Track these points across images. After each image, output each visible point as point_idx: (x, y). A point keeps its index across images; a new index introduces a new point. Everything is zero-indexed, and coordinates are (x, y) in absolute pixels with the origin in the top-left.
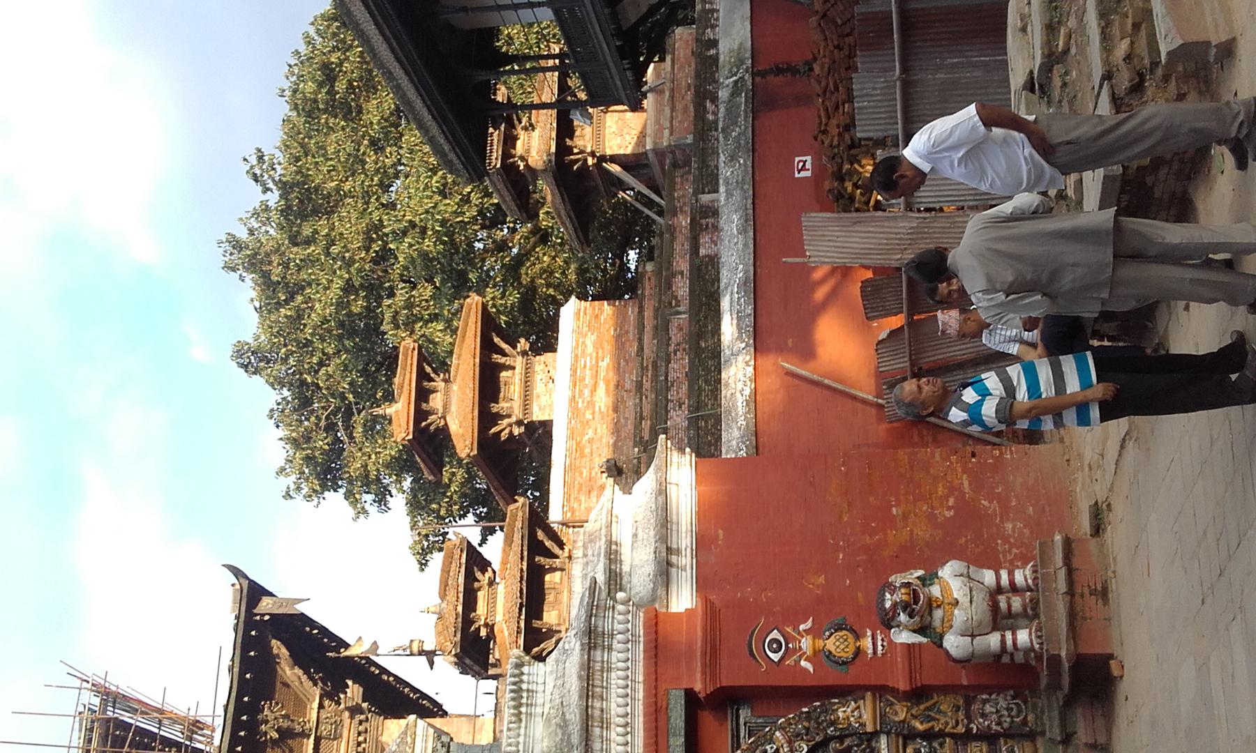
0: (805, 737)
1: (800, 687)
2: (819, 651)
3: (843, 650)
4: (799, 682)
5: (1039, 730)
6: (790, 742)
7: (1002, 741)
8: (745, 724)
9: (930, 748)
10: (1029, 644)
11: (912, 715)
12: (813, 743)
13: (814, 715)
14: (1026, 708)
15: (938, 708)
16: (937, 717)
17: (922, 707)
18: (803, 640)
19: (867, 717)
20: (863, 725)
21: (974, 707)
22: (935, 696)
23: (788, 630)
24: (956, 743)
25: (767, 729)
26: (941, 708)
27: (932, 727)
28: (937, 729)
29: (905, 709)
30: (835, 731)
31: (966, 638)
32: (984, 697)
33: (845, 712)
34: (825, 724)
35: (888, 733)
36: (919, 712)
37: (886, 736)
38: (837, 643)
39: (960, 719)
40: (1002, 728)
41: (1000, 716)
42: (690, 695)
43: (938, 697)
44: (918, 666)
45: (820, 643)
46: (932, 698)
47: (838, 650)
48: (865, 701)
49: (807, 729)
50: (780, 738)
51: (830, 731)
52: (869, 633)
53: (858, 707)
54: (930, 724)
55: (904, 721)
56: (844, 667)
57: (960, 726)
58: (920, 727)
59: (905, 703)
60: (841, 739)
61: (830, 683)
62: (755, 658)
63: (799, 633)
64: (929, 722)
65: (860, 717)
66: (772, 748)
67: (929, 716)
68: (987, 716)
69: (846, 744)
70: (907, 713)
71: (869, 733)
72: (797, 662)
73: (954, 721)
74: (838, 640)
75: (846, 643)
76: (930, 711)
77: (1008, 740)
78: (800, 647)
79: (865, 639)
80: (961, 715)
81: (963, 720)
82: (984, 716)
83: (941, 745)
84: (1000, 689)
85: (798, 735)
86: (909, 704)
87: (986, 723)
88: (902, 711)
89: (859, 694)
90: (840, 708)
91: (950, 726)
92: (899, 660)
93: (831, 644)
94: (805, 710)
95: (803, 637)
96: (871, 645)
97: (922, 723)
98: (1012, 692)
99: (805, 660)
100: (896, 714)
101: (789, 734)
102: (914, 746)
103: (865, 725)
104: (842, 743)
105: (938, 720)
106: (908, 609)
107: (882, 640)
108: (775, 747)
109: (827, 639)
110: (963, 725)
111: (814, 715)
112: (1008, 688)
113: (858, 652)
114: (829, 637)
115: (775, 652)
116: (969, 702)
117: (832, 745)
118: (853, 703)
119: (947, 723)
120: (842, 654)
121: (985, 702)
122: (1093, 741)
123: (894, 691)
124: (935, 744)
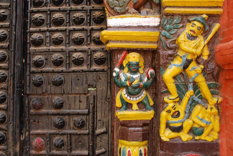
9: (138, 86)
16: (185, 100)
17: (201, 80)
26: (198, 108)
27: (168, 93)
28: (166, 99)
29: (199, 51)
37: (157, 24)
46: (213, 94)
55: (177, 48)
59: (206, 53)
64: (177, 87)
67: (187, 89)
70: (194, 54)
73: (179, 125)
86: (205, 58)
88: (197, 47)
97: (174, 78)
102: (141, 64)
110: (170, 139)
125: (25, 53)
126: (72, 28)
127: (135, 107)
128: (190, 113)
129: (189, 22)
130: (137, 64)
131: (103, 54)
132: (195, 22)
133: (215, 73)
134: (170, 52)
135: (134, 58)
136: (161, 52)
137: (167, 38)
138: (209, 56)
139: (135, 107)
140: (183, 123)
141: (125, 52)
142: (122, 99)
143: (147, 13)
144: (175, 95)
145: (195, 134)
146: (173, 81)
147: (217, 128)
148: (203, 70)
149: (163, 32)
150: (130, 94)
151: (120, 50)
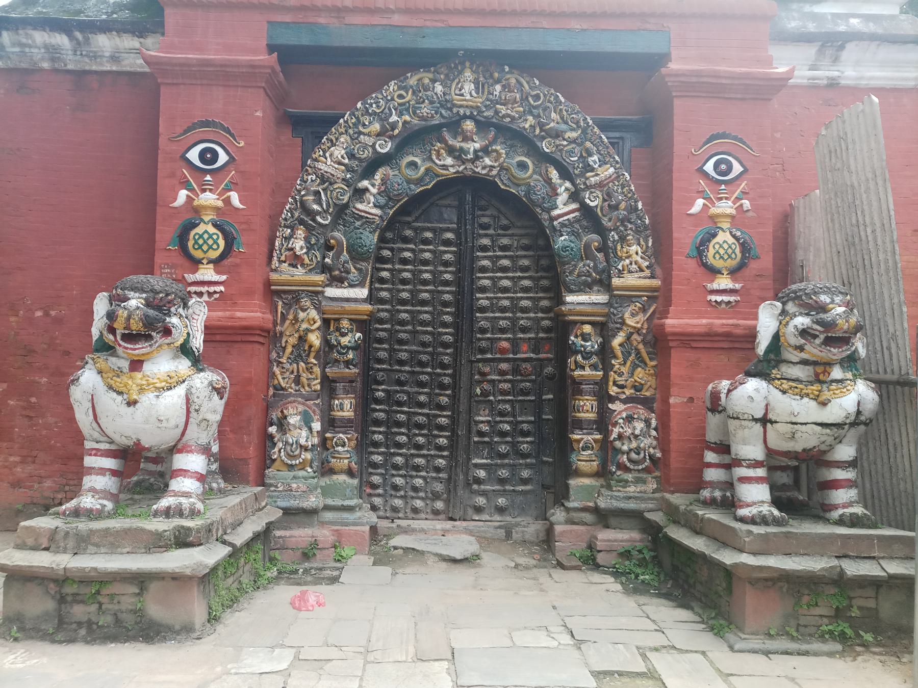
0: (606, 203)
1: (670, 199)
2: (715, 223)
3: (718, 252)
4: (676, 195)
5: (613, 482)
6: (600, 185)
7: (599, 437)
8: (621, 138)
10: (749, 500)
11: (632, 334)
12: (600, 214)
13: (633, 217)
14: (638, 471)
15: (640, 366)
16: (629, 363)
17: (641, 346)
18: (730, 203)
19: (631, 280)
20: (620, 273)
21: (642, 411)
22: (654, 363)
23: (743, 184)
24: (596, 383)
25: (617, 158)
26: (639, 369)
27: (615, 357)
28: (613, 362)
29: (639, 326)
30: (614, 241)
31: (763, 412)
32: (654, 423)
33: (637, 253)
34: (622, 229)
35: (609, 304)
36: (635, 343)
37: (606, 302)
38: (725, 246)
39: (626, 390)
40: (615, 440)
41: (630, 439)
42: (664, 58)
43: (652, 367)
44: (694, 345)
45: (726, 226)
46: (651, 359)
47: (717, 246)
48: (649, 278)
49: (616, 208)
50: (606, 173)
51: (613, 235)
52: (738, 286)
53: (642, 270)
54: (619, 354)
55: (623, 323)
56: (695, 253)
57: (615, 388)
58: (616, 342)
59: (646, 326)
60: (603, 248)
61: (675, 235)
62: (709, 141)
63: (738, 199)
65: (630, 272)
66: (595, 162)
67: (630, 354)
68: (630, 422)
69: (598, 255)
70: (635, 328)
71: (610, 282)
72: (701, 194)
73: (623, 383)
74: (730, 247)
75: (726, 257)
76: (636, 355)
77: (599, 444)
78: (721, 199)
79: (729, 280)
80: (629, 392)
81: (624, 393)
82: (630, 419)
83: (594, 367)
84: (663, 442)
85: (609, 195)
86: (644, 331)
87: (621, 421)
88: (638, 323)
89: (658, 271)
90: (642, 248)
91: (618, 378)
92: (704, 321)
93: (723, 237)
94: (640, 205)
95: (734, 203)
96: (723, 287)
97: (620, 345)
98: (659, 455)
99: (704, 205)
100: (633, 315)
101: (611, 185)
103: (619, 277)
104: (599, 250)
105: (625, 364)
106: (819, 328)
107: (729, 302)
108: (596, 166)
109: (731, 233)
110: (617, 393)
111: (633, 217)
112: (663, 451)
113: (714, 272)
114: (734, 236)
115: (716, 166)
116: (646, 403)
117: (595, 236)
118: (647, 263)
119: (621, 374)
120: (712, 251)
121: (647, 422)
122: (598, 549)
123: (664, 314)
124: (594, 359)
125: (472, 321)
126: (519, 295)
127: (587, 368)
128: (633, 374)
129: (634, 302)
130: (589, 334)
131: (550, 323)
132: (637, 304)
133: (652, 343)
134: (618, 326)
135: (587, 329)
136: (611, 325)
137: (615, 315)
138: (647, 329)
139: (587, 368)
140: (626, 381)
141: (579, 324)
142: (576, 362)
143: (599, 291)
144: (621, 360)
145: (636, 391)
146: (618, 348)
147: (654, 386)
148: (642, 341)
149: (612, 310)
150: (584, 358)
151: (575, 323)
